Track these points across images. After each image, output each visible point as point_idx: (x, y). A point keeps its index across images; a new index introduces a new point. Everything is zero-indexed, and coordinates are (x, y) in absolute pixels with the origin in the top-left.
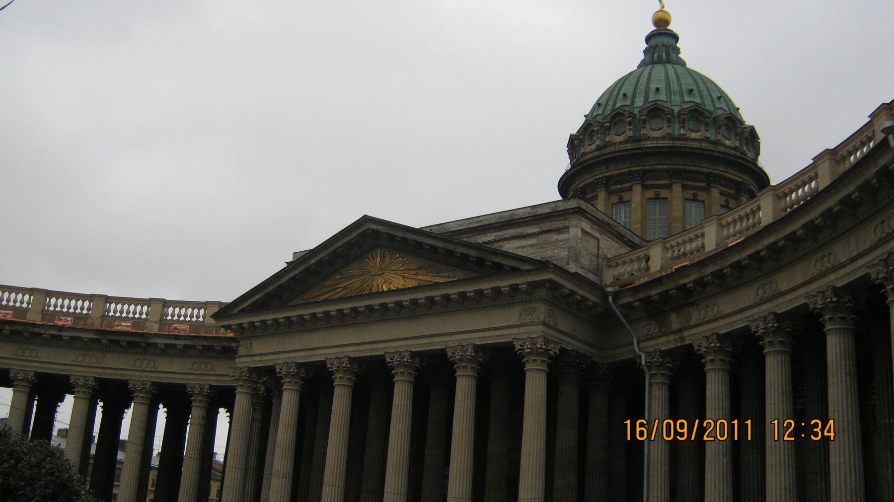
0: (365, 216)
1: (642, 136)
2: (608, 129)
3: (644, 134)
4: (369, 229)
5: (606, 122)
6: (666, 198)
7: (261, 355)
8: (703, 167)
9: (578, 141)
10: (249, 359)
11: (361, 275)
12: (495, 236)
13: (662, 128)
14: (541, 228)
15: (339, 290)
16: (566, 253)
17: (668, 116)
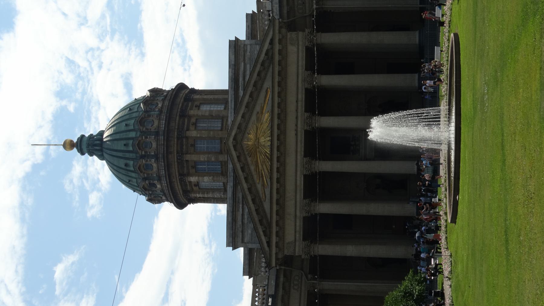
1: (155, 130)
2: (146, 152)
3: (155, 129)
4: (233, 142)
5: (142, 153)
6: (197, 119)
7: (295, 232)
8: (180, 101)
9: (147, 181)
10: (297, 243)
11: (257, 154)
12: (242, 90)
14: (242, 62)
15: (263, 172)
16: (258, 46)
17: (146, 116)
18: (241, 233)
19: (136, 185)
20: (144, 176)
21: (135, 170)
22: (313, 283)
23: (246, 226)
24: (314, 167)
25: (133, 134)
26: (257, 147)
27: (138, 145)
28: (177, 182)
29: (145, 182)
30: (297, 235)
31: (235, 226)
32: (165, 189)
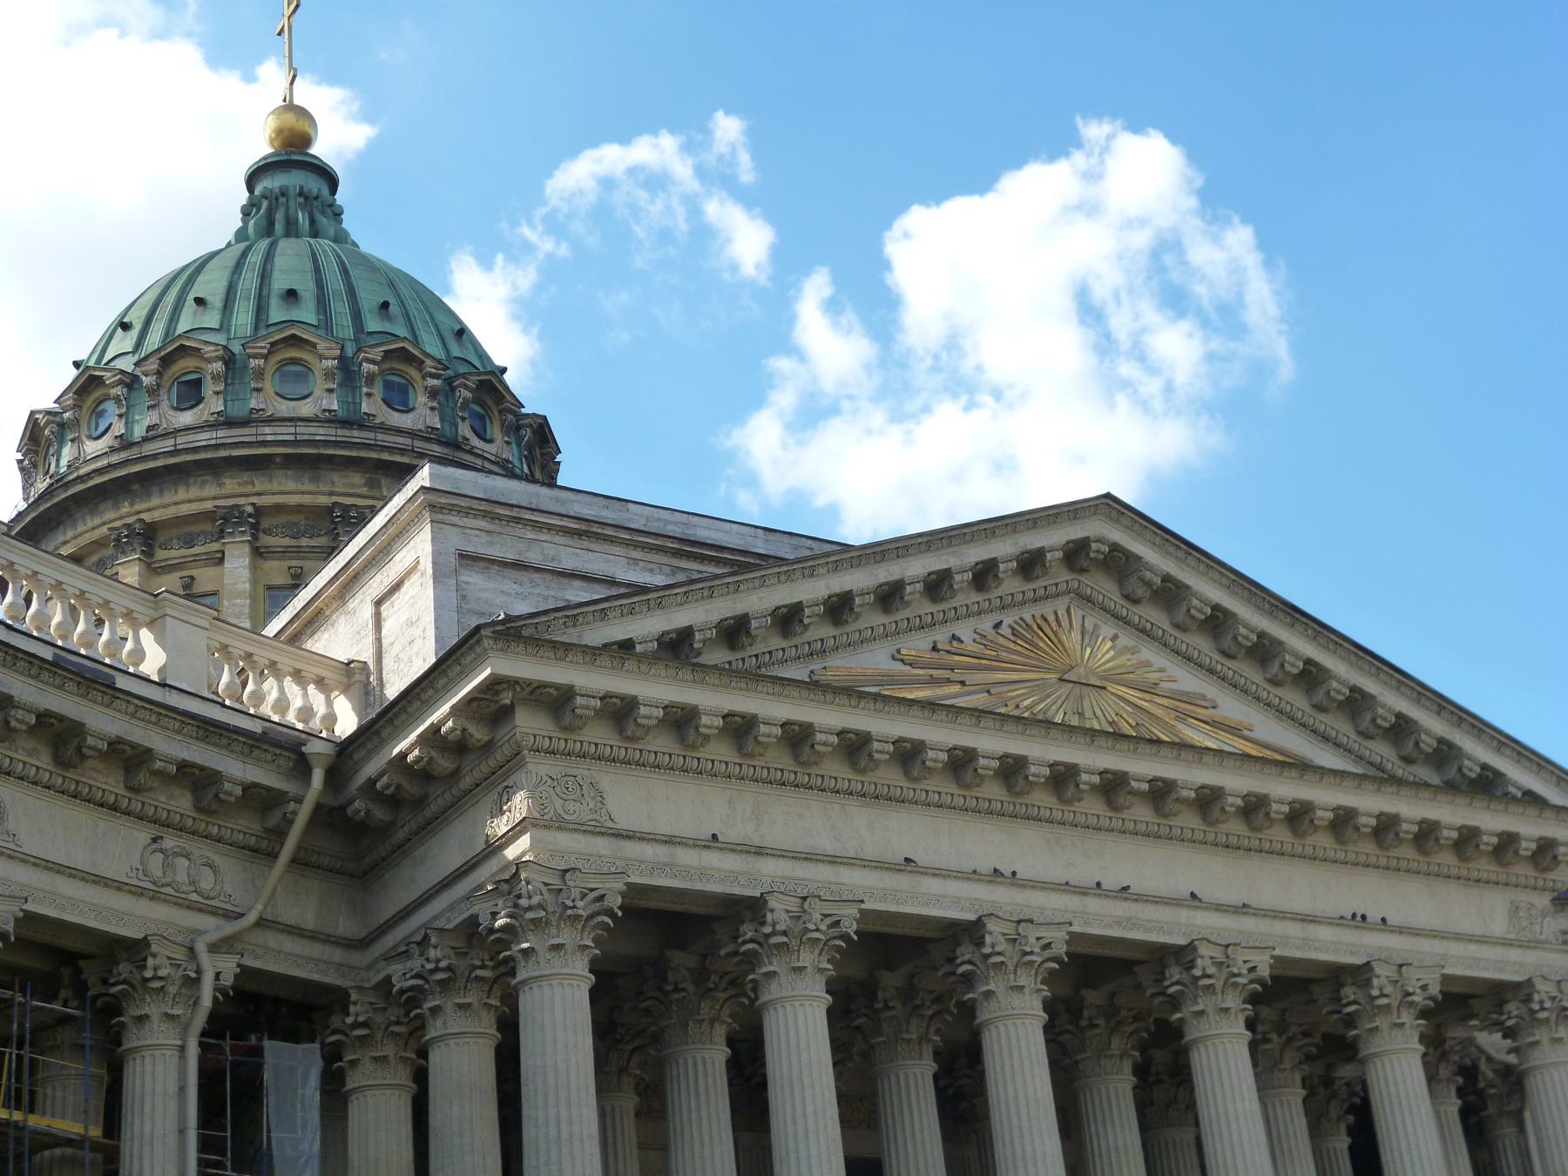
0: (1108, 496)
5: (368, 360)
7: (670, 841)
10: (602, 845)
13: (490, 441)
18: (511, 556)
19: (181, 328)
20: (255, 356)
21: (268, 326)
22: (194, 982)
23: (551, 593)
24: (1021, 988)
25: (432, 346)
26: (1065, 677)
27: (405, 356)
28: (214, 498)
29: (218, 358)
30: (649, 851)
31: (550, 528)
32: (182, 441)
